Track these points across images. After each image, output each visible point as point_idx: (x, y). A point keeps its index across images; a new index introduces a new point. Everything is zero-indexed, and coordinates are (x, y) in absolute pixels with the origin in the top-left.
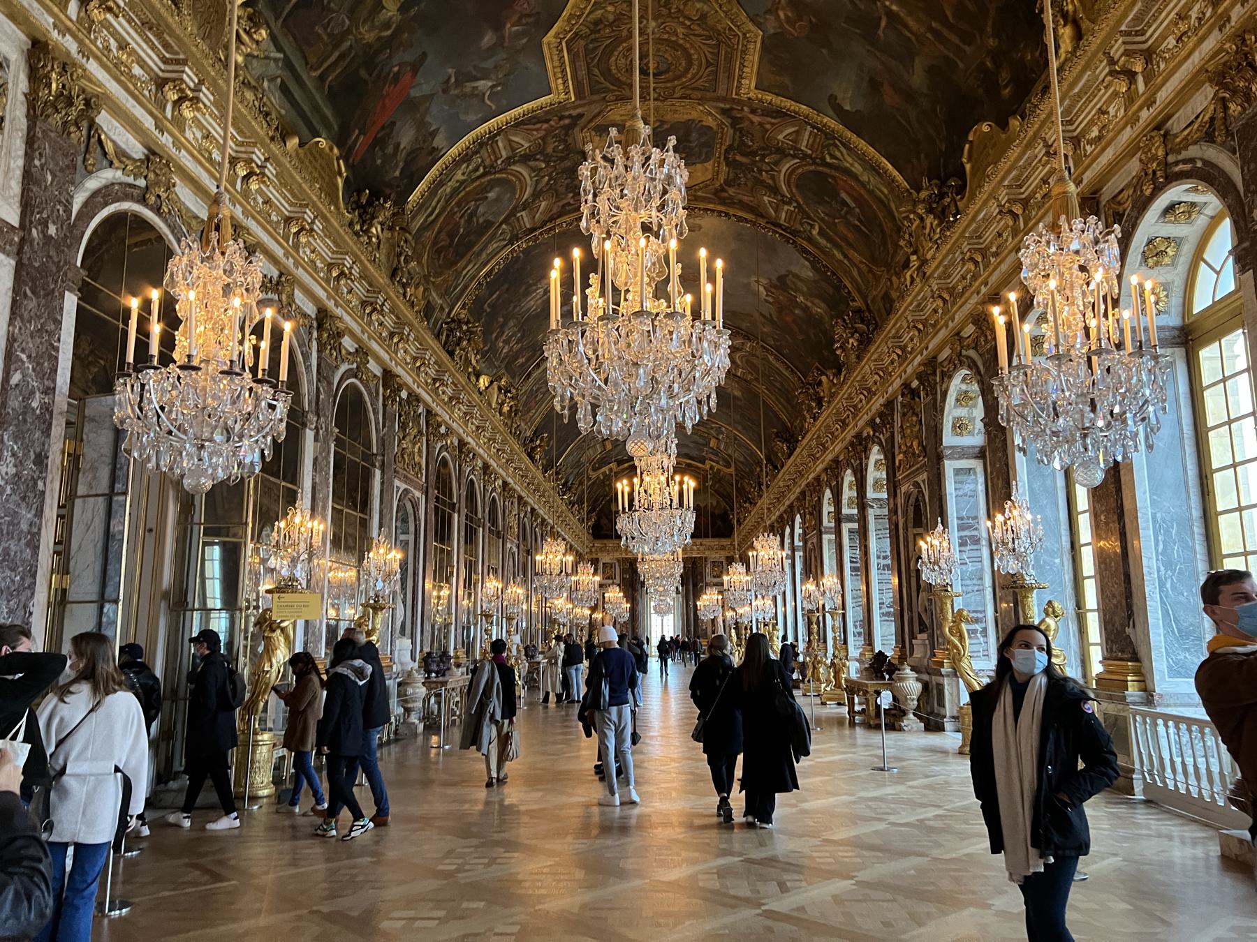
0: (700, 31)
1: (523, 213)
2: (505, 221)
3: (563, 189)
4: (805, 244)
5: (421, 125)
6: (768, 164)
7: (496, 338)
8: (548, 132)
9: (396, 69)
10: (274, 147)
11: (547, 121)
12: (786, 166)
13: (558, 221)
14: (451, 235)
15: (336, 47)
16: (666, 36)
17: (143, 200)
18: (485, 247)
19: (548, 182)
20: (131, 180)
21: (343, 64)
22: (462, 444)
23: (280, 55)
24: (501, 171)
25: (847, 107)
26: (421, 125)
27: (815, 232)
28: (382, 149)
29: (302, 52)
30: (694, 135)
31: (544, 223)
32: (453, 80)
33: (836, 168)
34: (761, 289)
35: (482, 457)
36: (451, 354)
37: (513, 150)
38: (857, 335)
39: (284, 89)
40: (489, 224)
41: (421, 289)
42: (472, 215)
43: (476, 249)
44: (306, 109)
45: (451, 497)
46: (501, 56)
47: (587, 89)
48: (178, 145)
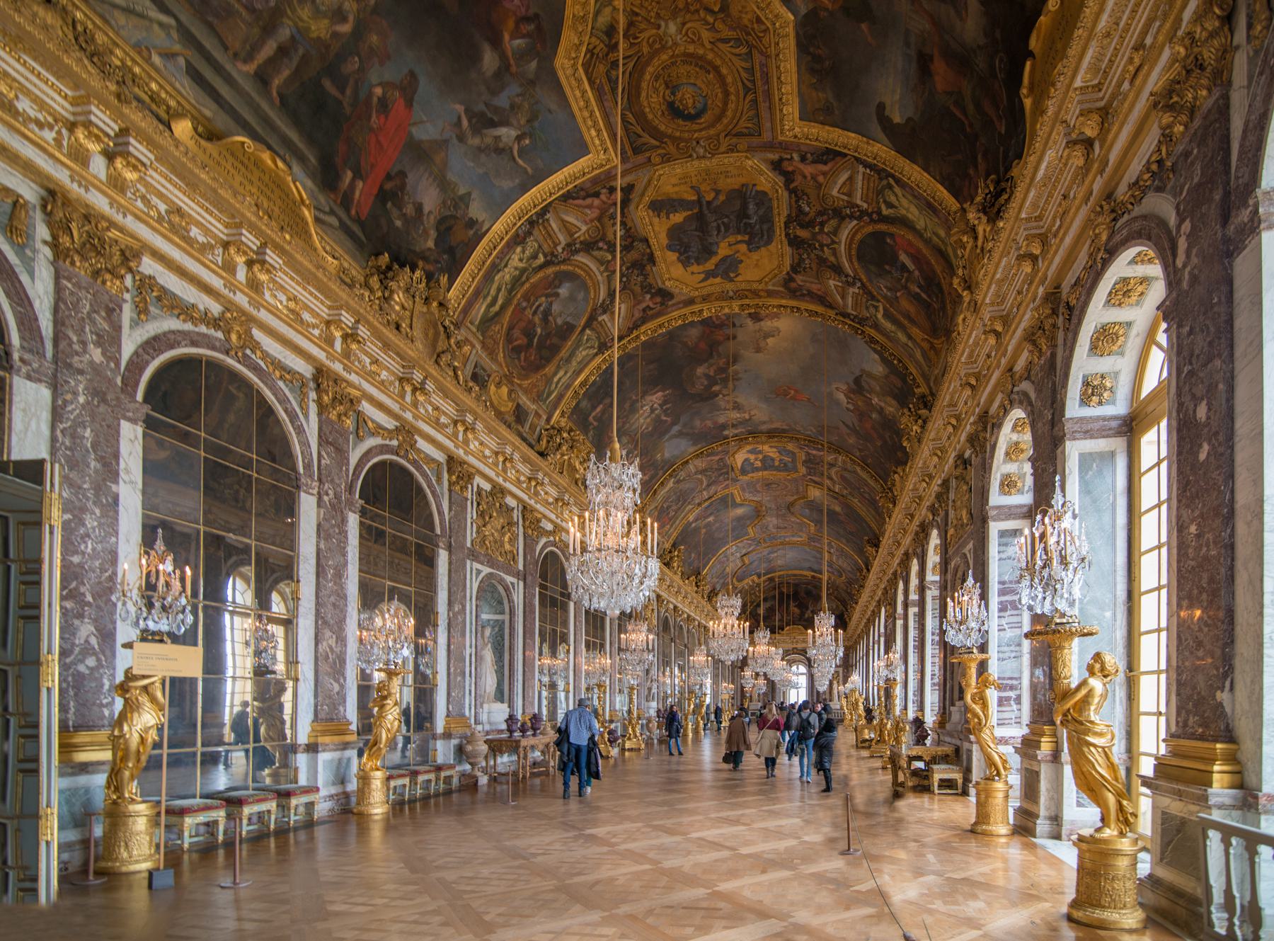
0: (727, 33)
1: (605, 317)
2: (588, 325)
3: (637, 289)
5: (444, 185)
13: (643, 329)
24: (564, 261)
26: (444, 185)
31: (630, 330)
37: (571, 235)
40: (568, 329)
43: (564, 353)
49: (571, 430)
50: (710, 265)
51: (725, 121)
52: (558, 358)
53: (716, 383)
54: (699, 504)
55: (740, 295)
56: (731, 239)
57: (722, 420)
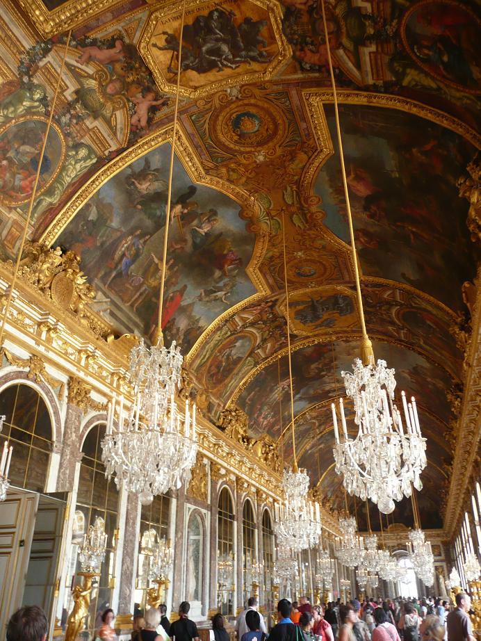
1: (259, 350)
4: (419, 350)
5: (190, 317)
6: (385, 310)
7: (258, 417)
8: (262, 311)
9: (171, 295)
10: (101, 343)
11: (260, 305)
12: (394, 310)
13: (280, 352)
14: (218, 367)
15: (137, 291)
16: (308, 258)
17: (27, 377)
18: (239, 371)
19: (269, 334)
20: (21, 369)
21: (143, 297)
22: (238, 479)
23: (109, 300)
25: (412, 278)
26: (190, 317)
27: (422, 343)
28: (170, 332)
29: (120, 296)
30: (340, 301)
31: (273, 354)
32: (203, 294)
33: (421, 309)
34: (406, 375)
35: (254, 486)
36: (222, 429)
38: (459, 399)
39: (112, 314)
40: (239, 359)
41: (204, 396)
42: (228, 356)
43: (235, 371)
44: (125, 320)
45: (231, 511)
46: (226, 280)
47: (277, 288)
48: (48, 349)
49: (236, 410)
50: (319, 322)
51: (325, 276)
52: (231, 375)
53: (324, 371)
54: (313, 438)
55: (336, 333)
56: (330, 312)
57: (327, 388)
